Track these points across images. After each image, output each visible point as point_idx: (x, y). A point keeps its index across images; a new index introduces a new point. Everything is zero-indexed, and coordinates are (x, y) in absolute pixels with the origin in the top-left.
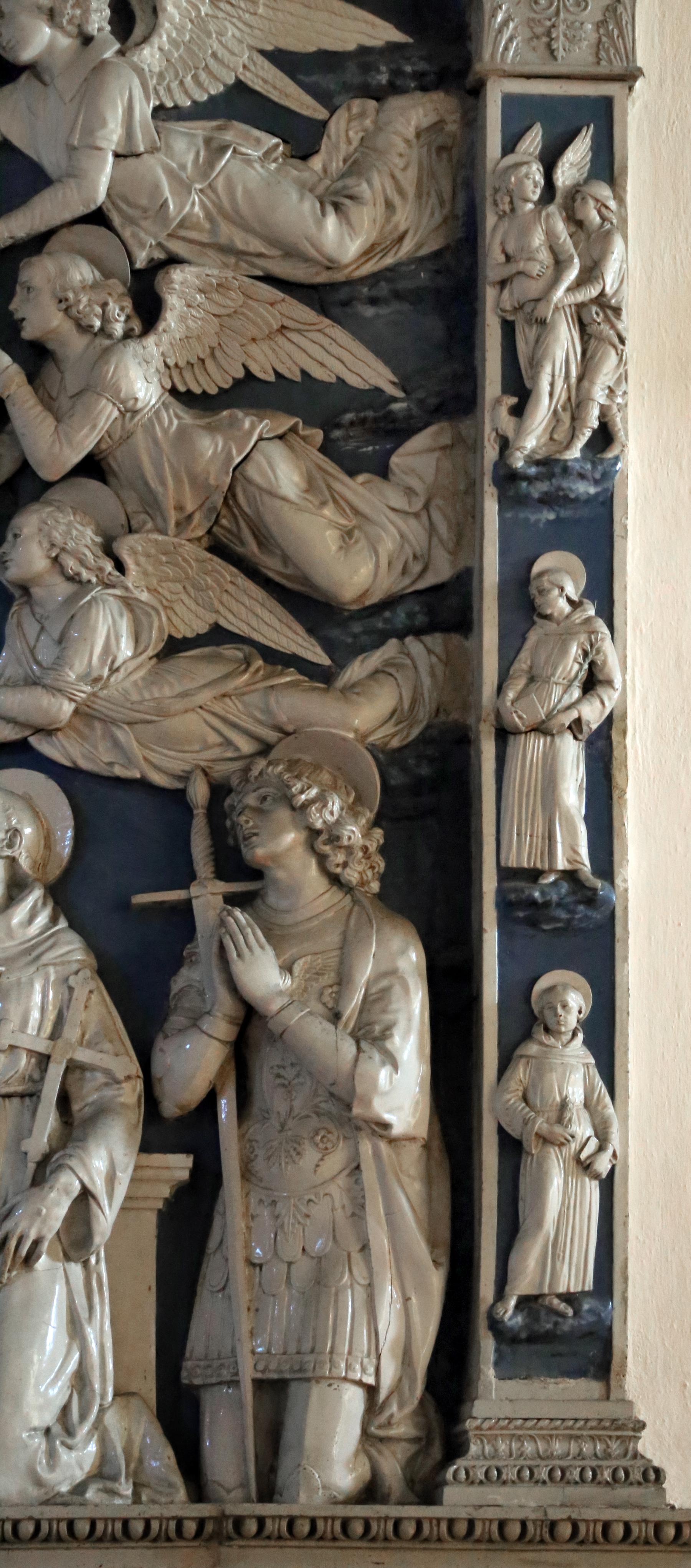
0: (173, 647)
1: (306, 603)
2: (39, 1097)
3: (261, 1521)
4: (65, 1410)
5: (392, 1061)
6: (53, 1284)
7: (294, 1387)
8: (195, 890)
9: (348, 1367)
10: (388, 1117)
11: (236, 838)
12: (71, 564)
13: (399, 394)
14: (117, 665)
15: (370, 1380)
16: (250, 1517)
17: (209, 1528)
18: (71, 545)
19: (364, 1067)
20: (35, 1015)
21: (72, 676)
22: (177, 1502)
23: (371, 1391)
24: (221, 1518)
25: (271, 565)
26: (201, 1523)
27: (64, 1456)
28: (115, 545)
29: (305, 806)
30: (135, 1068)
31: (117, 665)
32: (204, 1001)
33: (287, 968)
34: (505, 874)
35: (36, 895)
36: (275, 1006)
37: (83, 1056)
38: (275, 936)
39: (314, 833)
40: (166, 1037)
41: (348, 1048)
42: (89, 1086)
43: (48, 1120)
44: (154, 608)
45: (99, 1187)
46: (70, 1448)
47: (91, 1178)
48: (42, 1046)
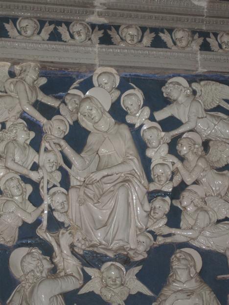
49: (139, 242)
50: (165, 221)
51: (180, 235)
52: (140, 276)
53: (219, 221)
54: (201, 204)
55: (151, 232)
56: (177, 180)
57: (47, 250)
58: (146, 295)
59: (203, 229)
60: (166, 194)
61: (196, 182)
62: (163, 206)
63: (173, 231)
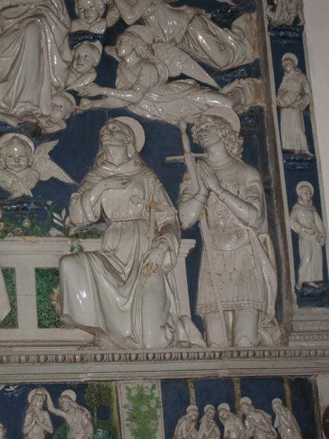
13: (233, 4)
34: (285, 152)
49: (54, 107)
50: (93, 76)
51: (114, 98)
52: (54, 155)
53: (171, 80)
54: (146, 54)
55: (74, 93)
56: (113, 17)
59: (148, 90)
60: (96, 37)
61: (140, 22)
62: (91, 55)
63: (104, 91)
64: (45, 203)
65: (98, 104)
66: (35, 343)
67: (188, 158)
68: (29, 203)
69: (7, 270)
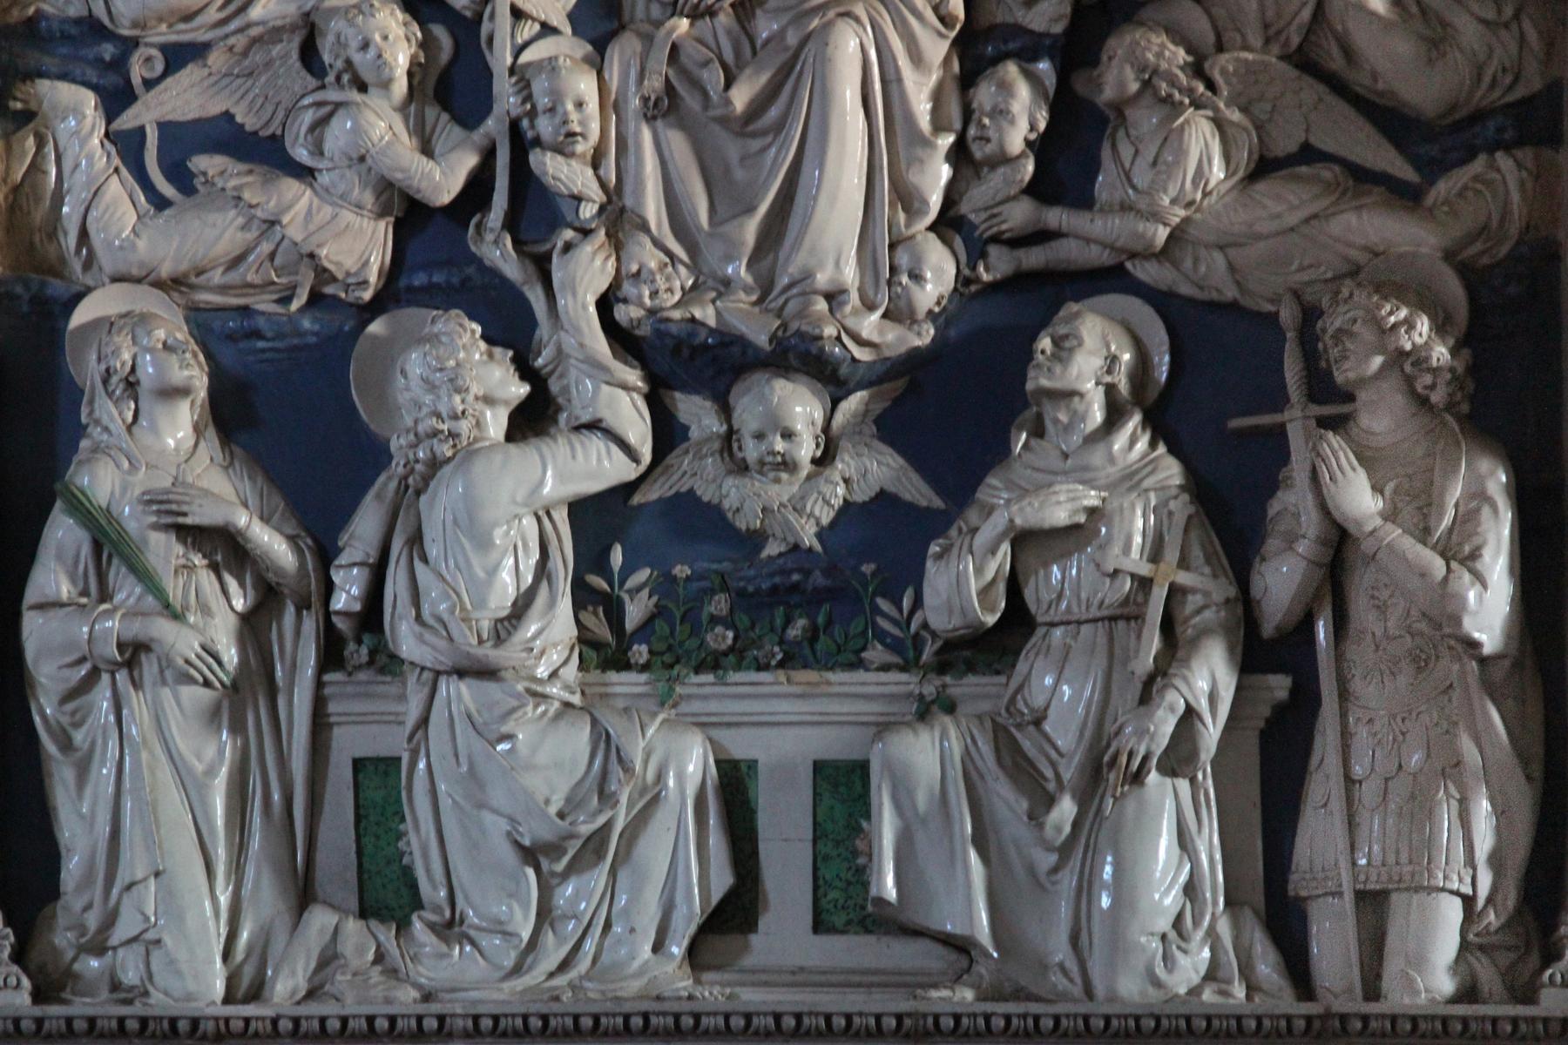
0: (1263, 168)
1: (1389, 119)
2: (1144, 620)
3: (1365, 1019)
4: (1179, 918)
5: (1480, 579)
6: (1164, 797)
7: (1394, 897)
8: (1287, 415)
9: (1445, 878)
10: (1476, 635)
11: (1328, 360)
12: (1164, 88)
14: (1209, 187)
15: (1468, 890)
16: (1356, 1015)
17: (1317, 1024)
18: (1164, 65)
19: (1453, 586)
20: (1138, 539)
21: (1166, 201)
22: (1286, 1002)
23: (1468, 901)
24: (1327, 1016)
25: (1359, 80)
26: (1309, 1019)
27: (1182, 960)
28: (1207, 65)
29: (1395, 326)
30: (1232, 591)
31: (1209, 187)
32: (1299, 524)
33: (1377, 489)
35: (1135, 420)
36: (1369, 528)
37: (1184, 578)
38: (1366, 459)
39: (1402, 354)
40: (1263, 559)
41: (1438, 565)
42: (1189, 608)
43: (1153, 643)
44: (1245, 129)
45: (1203, 705)
46: (1185, 952)
47: (1195, 697)
48: (1145, 569)
52: (890, 428)
57: (511, 328)
58: (911, 507)
63: (1056, 217)
64: (856, 569)
65: (1034, 258)
66: (799, 978)
67: (1296, 420)
68: (807, 573)
69: (735, 764)
